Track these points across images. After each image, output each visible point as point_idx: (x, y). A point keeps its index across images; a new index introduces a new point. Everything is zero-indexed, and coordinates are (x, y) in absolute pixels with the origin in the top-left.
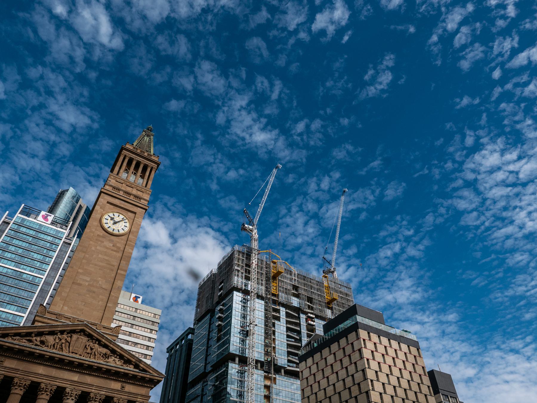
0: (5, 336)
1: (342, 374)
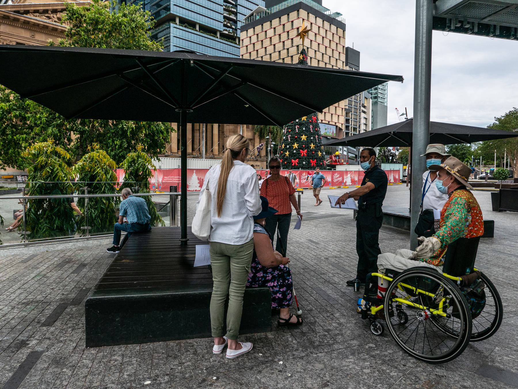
0: (27, 12)
1: (279, 47)
